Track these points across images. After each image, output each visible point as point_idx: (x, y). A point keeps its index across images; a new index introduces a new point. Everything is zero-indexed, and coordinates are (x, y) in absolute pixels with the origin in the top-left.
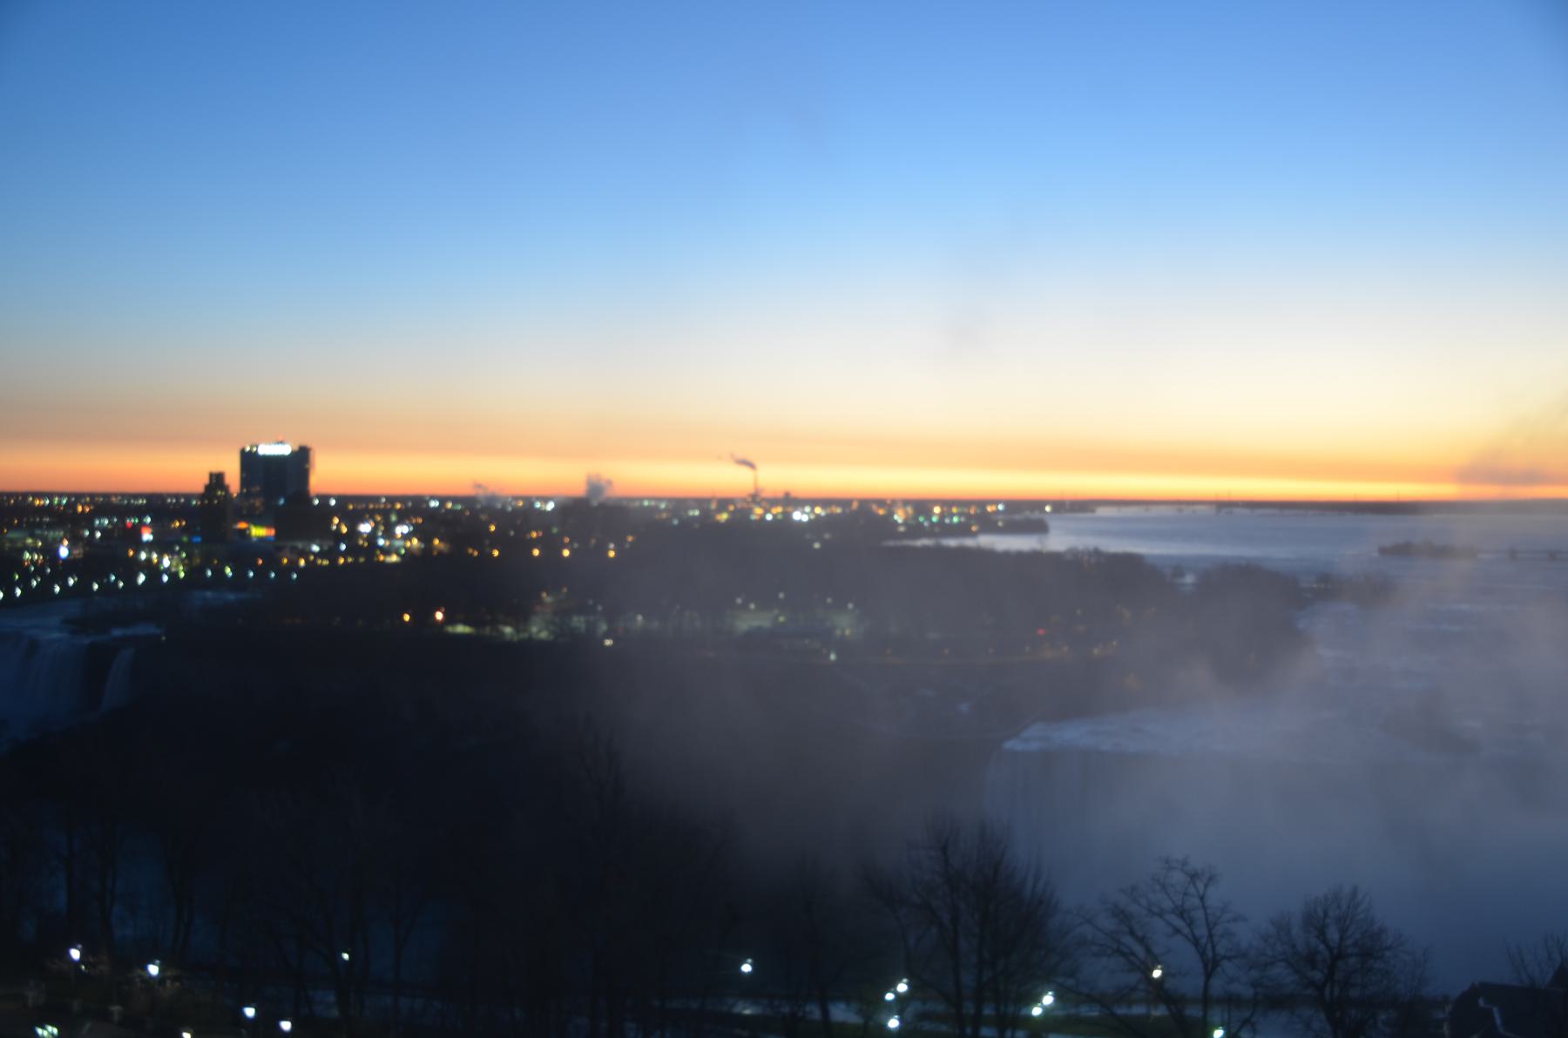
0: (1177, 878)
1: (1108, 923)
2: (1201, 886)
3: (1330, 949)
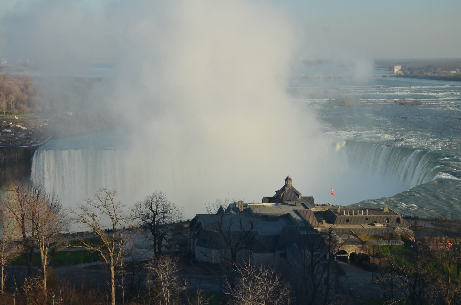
0: (104, 194)
1: (79, 212)
2: (111, 196)
3: (154, 212)
